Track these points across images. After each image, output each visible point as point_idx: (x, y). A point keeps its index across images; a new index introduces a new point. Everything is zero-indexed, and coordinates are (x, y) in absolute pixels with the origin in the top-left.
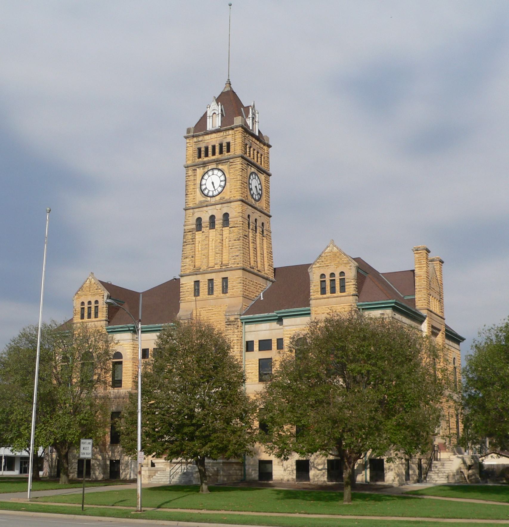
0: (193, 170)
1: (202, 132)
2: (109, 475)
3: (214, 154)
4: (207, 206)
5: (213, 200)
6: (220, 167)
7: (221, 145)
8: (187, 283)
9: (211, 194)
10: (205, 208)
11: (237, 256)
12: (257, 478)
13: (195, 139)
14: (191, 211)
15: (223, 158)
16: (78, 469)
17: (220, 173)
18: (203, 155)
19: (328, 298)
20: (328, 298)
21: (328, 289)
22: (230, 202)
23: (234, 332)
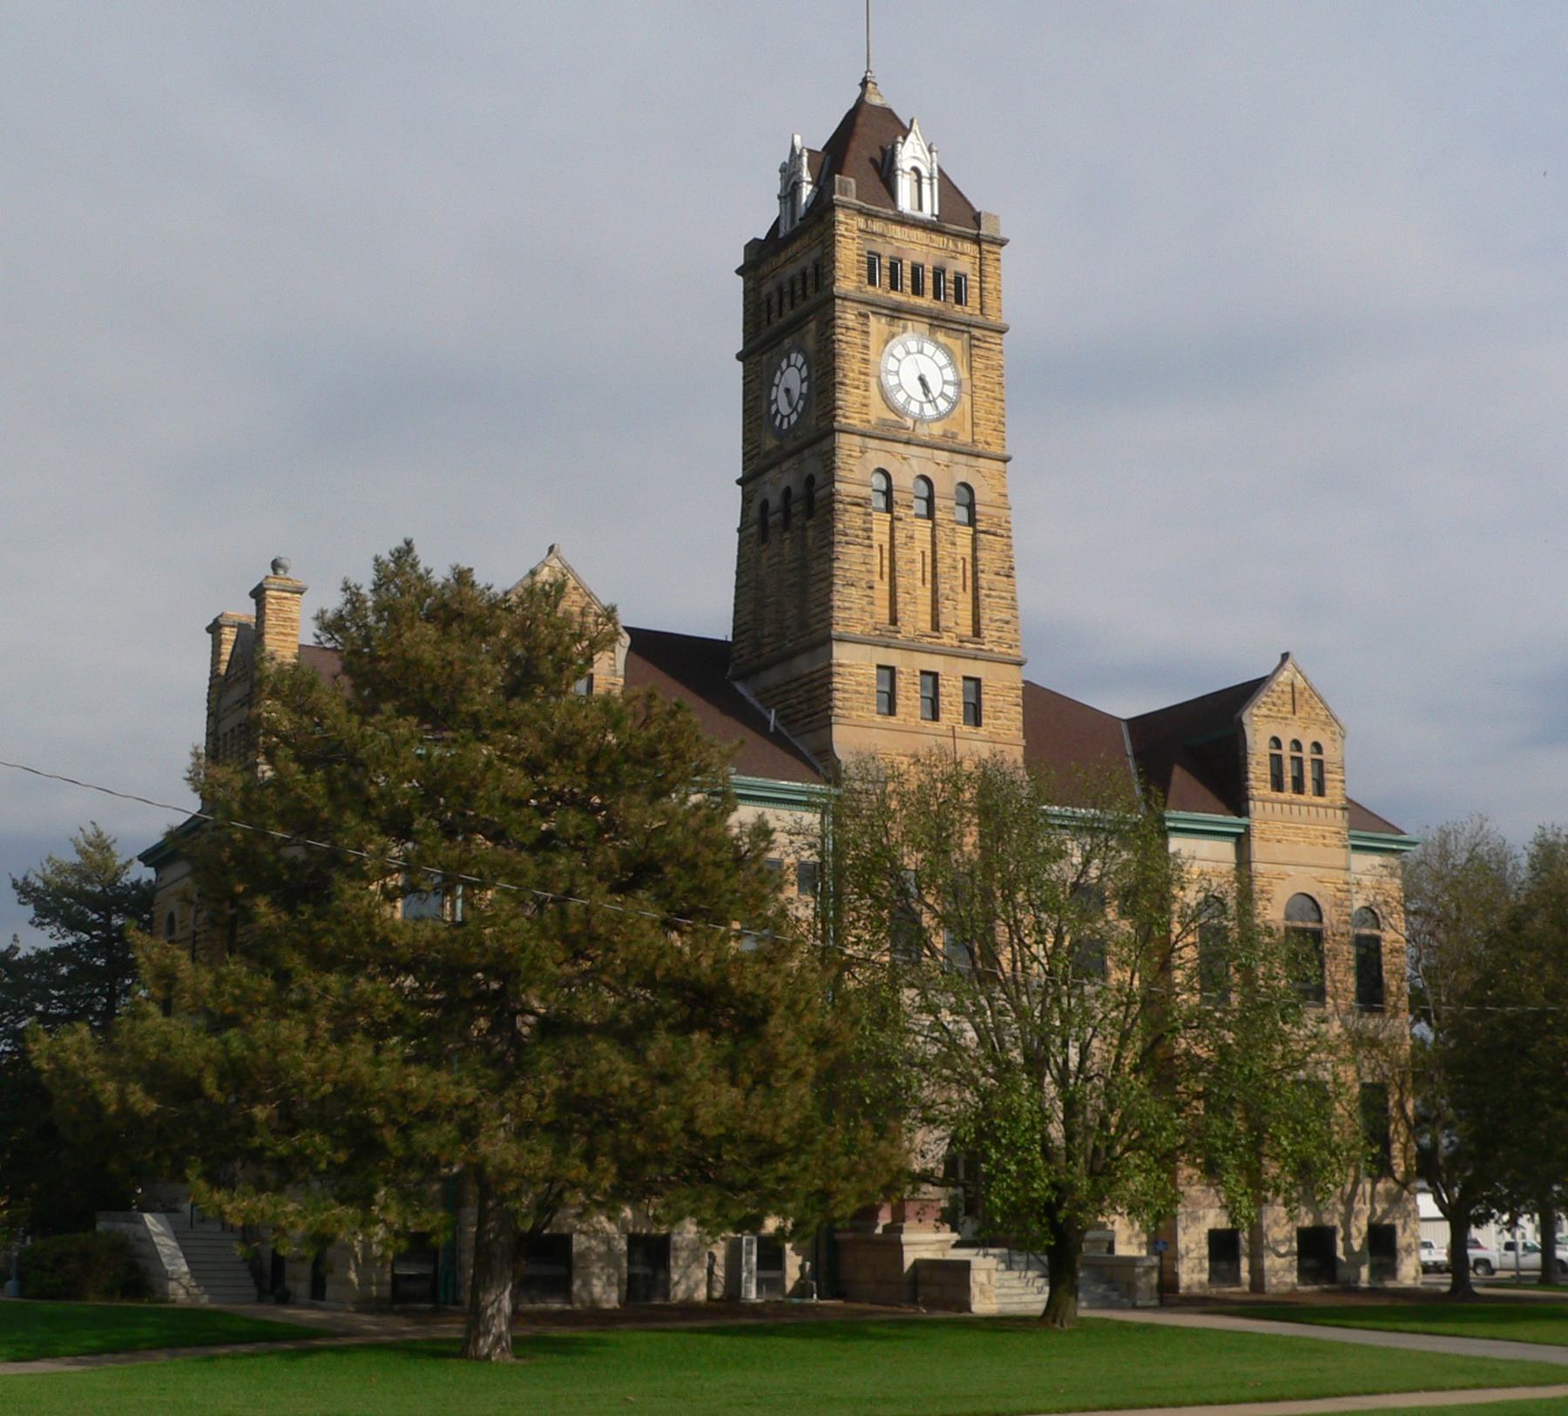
0: (860, 314)
4: (908, 443)
7: (938, 273)
10: (900, 448)
13: (861, 222)
14: (857, 440)
17: (942, 359)
19: (1290, 803)
20: (1290, 803)
21: (1309, 783)
22: (978, 456)
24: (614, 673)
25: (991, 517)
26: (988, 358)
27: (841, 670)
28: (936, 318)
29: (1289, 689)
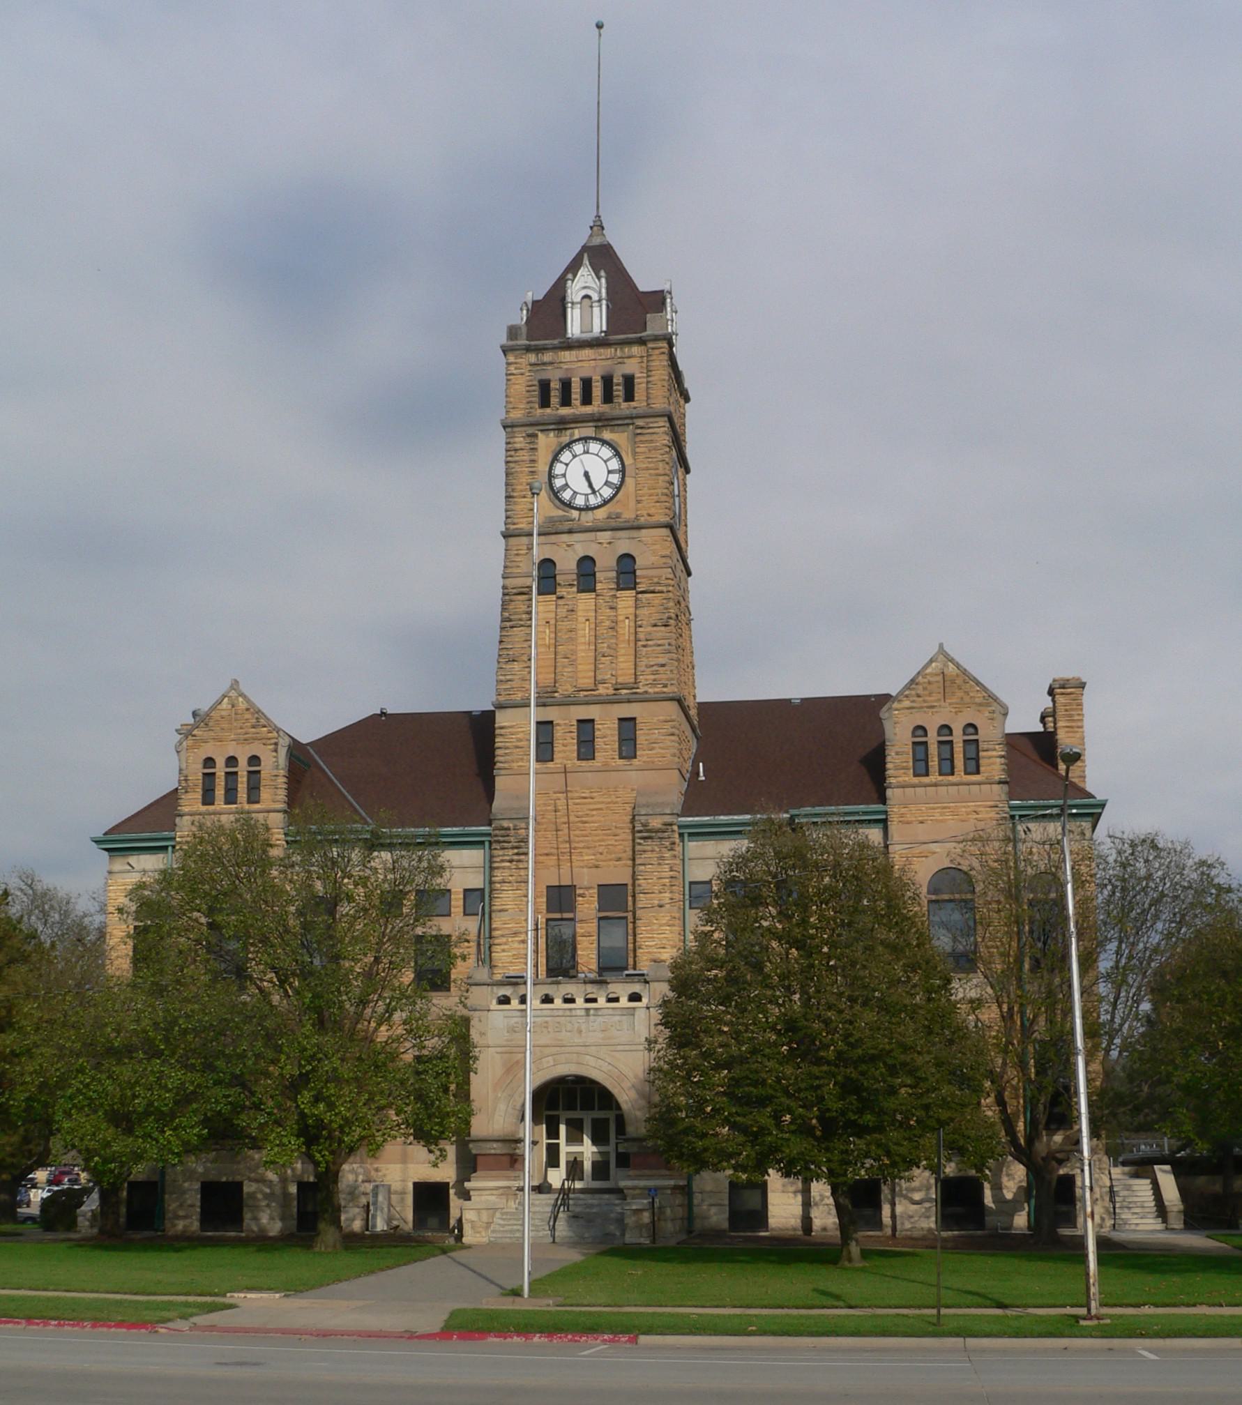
0: (529, 436)
1: (556, 342)
2: (295, 1222)
3: (587, 400)
4: (570, 532)
5: (587, 518)
6: (607, 435)
7: (608, 381)
8: (516, 729)
9: (580, 501)
10: (565, 537)
11: (663, 665)
12: (726, 1225)
13: (532, 358)
15: (617, 413)
16: (202, 1207)
17: (607, 452)
18: (555, 399)
19: (935, 785)
20: (935, 785)
22: (639, 528)
23: (662, 858)
24: (277, 768)
25: (650, 578)
26: (652, 441)
27: (502, 731)
28: (599, 420)
29: (940, 678)
